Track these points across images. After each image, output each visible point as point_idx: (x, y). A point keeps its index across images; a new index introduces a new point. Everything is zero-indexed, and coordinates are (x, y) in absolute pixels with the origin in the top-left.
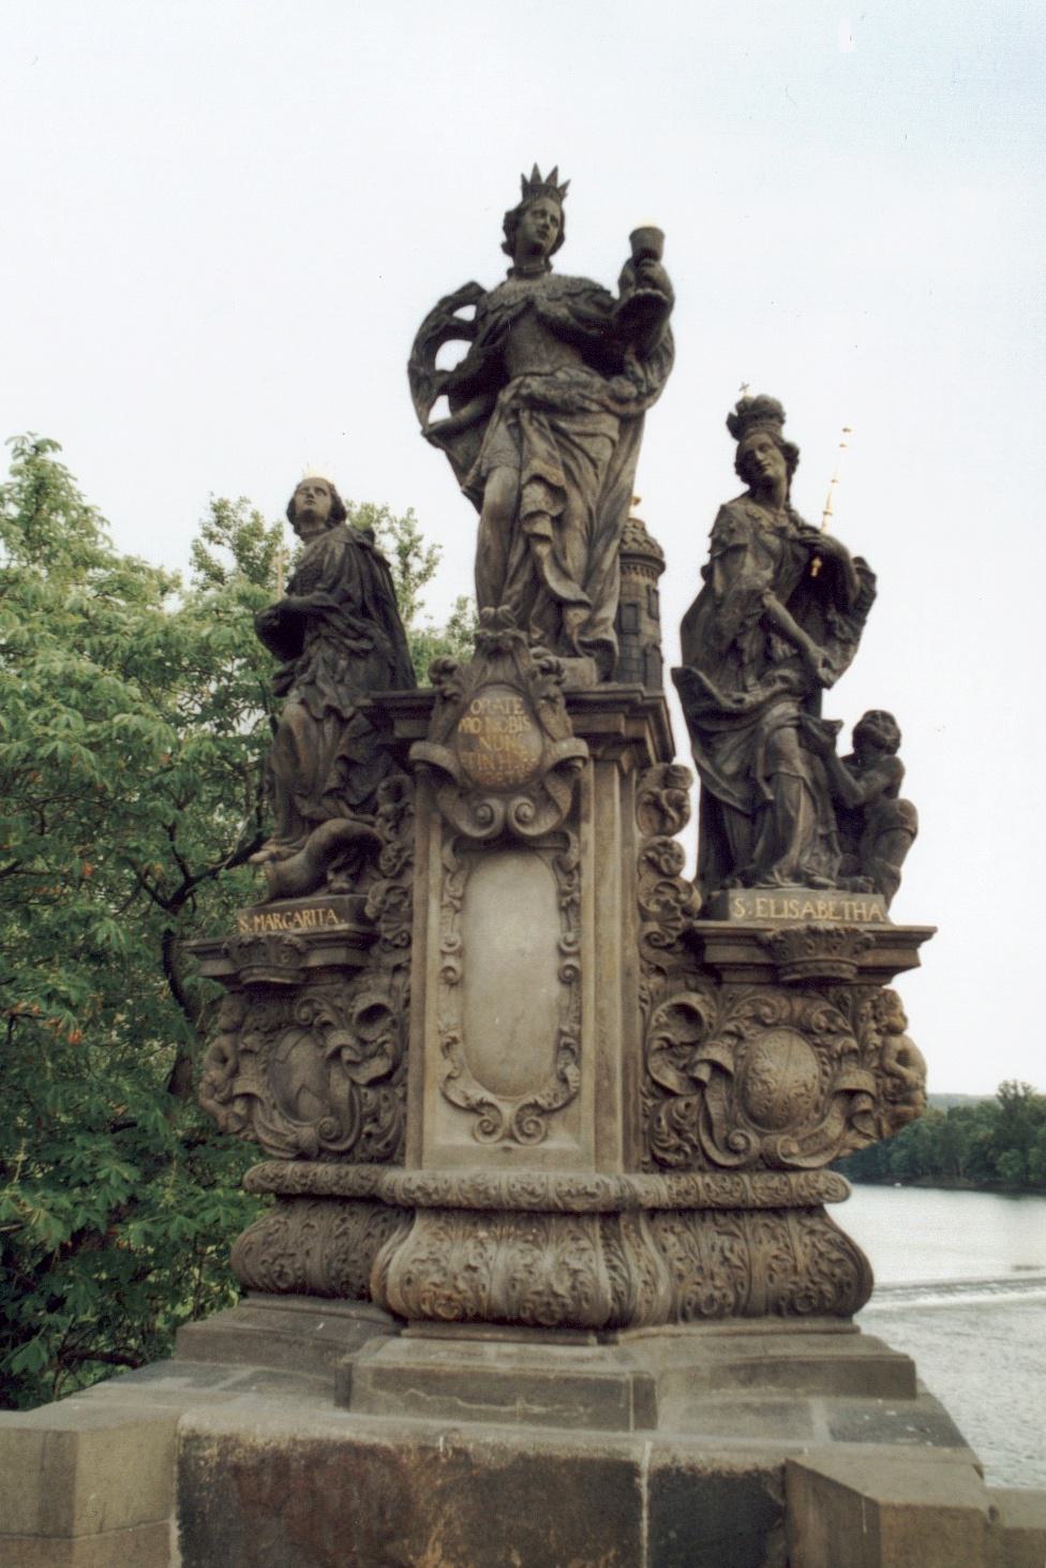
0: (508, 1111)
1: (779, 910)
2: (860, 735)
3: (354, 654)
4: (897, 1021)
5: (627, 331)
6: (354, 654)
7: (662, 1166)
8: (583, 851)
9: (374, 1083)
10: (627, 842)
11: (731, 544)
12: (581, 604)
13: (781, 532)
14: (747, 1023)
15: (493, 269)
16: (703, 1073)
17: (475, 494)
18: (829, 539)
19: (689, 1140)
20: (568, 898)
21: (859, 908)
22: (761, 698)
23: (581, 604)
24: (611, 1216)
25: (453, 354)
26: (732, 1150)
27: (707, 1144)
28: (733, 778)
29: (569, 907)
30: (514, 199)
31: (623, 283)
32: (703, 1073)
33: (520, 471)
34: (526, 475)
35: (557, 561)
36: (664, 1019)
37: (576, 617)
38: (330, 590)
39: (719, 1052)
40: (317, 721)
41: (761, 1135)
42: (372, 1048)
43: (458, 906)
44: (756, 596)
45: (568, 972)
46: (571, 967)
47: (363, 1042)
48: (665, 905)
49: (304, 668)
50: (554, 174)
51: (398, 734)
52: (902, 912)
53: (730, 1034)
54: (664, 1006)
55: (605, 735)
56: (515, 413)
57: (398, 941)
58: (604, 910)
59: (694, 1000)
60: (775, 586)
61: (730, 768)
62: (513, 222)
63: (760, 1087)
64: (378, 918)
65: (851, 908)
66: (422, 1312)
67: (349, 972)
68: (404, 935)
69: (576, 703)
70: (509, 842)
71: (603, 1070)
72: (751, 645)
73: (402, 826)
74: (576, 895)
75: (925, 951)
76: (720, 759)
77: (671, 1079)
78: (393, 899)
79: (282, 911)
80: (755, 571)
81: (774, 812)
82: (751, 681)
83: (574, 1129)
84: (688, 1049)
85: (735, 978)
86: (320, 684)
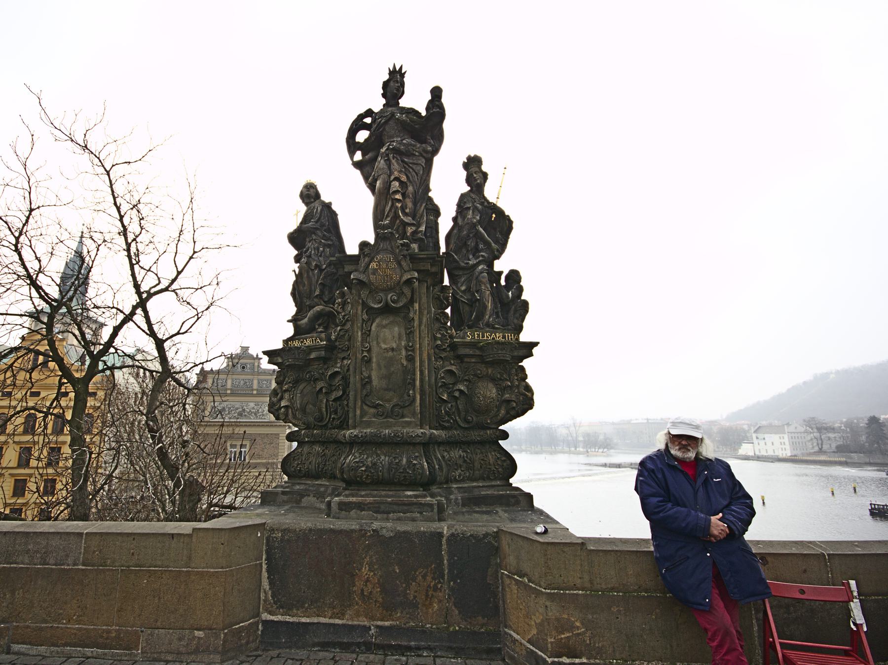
0: (388, 406)
2: (507, 278)
3: (325, 246)
5: (428, 127)
6: (325, 246)
7: (443, 428)
8: (415, 313)
9: (335, 400)
10: (429, 312)
12: (412, 225)
15: (378, 104)
16: (457, 394)
17: (372, 187)
23: (412, 225)
24: (427, 445)
25: (362, 136)
26: (468, 422)
28: (464, 292)
29: (410, 334)
30: (386, 77)
31: (427, 109)
32: (457, 394)
33: (390, 176)
34: (392, 178)
35: (403, 209)
37: (410, 230)
38: (316, 222)
40: (312, 270)
41: (477, 416)
42: (334, 388)
43: (367, 334)
44: (474, 225)
47: (331, 385)
48: (443, 335)
49: (306, 252)
50: (401, 68)
51: (346, 270)
52: (524, 337)
55: (424, 271)
56: (387, 155)
58: (422, 335)
59: (453, 368)
61: (463, 288)
62: (385, 85)
64: (336, 340)
69: (413, 258)
70: (387, 310)
72: (471, 243)
75: (535, 350)
76: (459, 285)
78: (341, 333)
79: (299, 339)
82: (471, 257)
83: (414, 414)
85: (468, 360)
86: (313, 256)
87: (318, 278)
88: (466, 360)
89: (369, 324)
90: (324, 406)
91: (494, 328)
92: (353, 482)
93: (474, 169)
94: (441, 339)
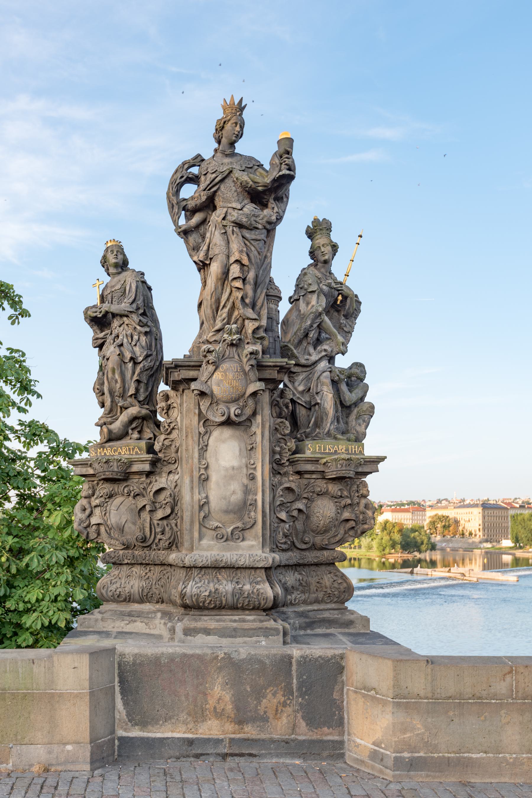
1: (325, 449)
4: (363, 491)
11: (308, 291)
13: (329, 285)
14: (311, 494)
16: (295, 513)
18: (347, 287)
19: (289, 539)
20: (251, 446)
21: (355, 448)
22: (317, 358)
27: (295, 541)
32: (295, 513)
36: (281, 493)
39: (300, 505)
43: (204, 449)
45: (251, 476)
46: (252, 473)
52: (371, 447)
53: (305, 498)
54: (282, 487)
57: (170, 461)
60: (324, 310)
63: (316, 518)
65: (352, 448)
66: (199, 606)
67: (149, 474)
68: (173, 459)
71: (263, 512)
72: (313, 335)
73: (169, 412)
74: (254, 445)
75: (381, 466)
77: (283, 515)
78: (167, 443)
80: (317, 303)
81: (319, 407)
83: (256, 537)
84: (289, 504)
87: (134, 373)
88: (307, 476)
89: (206, 438)
90: (148, 525)
91: (335, 438)
92: (193, 607)
93: (321, 240)
94: (280, 453)
